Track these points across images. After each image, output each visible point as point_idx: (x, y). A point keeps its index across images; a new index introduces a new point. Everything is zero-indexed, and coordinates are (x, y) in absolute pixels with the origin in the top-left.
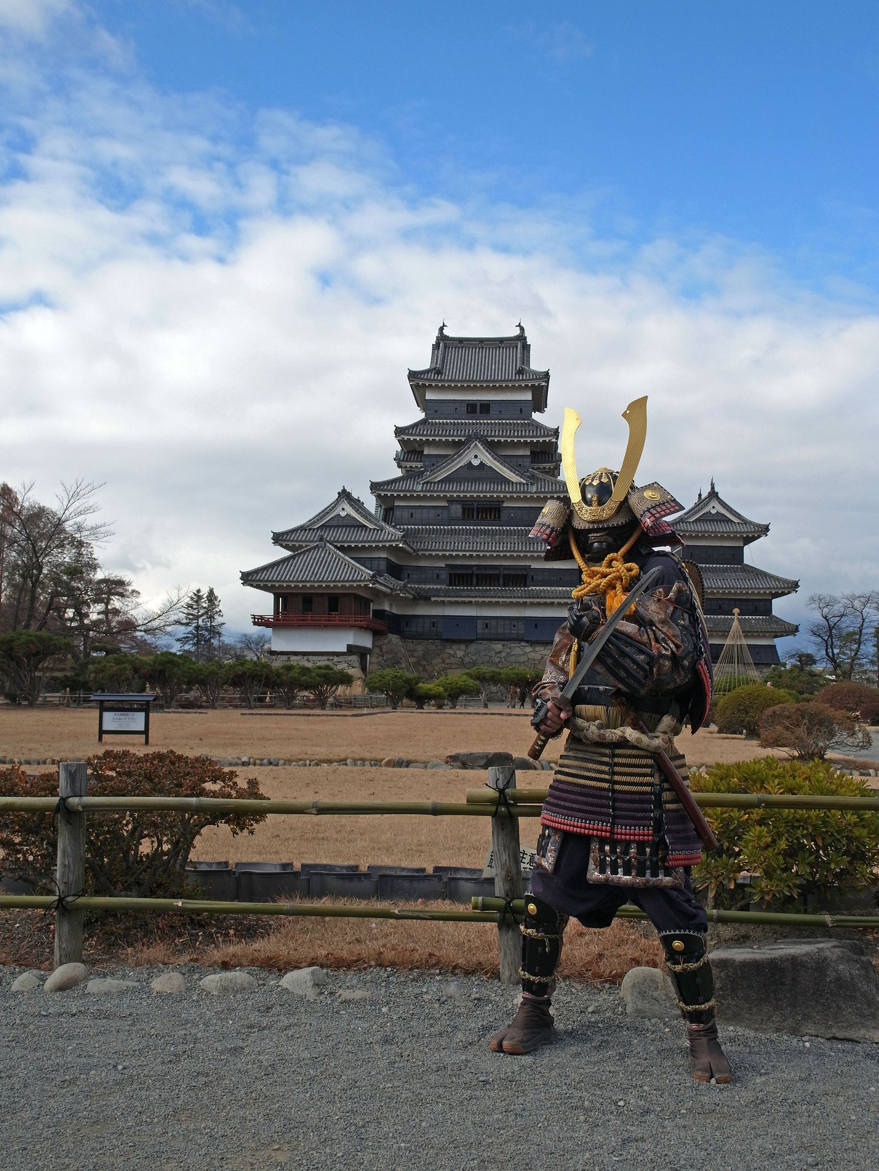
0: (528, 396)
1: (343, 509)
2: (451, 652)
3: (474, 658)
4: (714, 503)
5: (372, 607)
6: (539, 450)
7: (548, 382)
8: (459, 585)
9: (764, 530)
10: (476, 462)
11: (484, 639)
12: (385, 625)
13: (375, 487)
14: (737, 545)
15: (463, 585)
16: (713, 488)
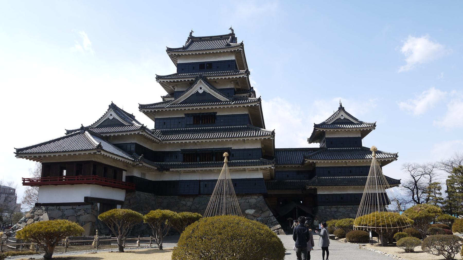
0: (233, 58)
1: (111, 115)
2: (184, 203)
3: (198, 206)
4: (342, 113)
5: (124, 174)
6: (240, 87)
7: (243, 48)
8: (189, 162)
9: (374, 126)
10: (201, 91)
11: (204, 195)
12: (133, 185)
13: (142, 108)
14: (357, 136)
15: (192, 162)
16: (341, 105)
